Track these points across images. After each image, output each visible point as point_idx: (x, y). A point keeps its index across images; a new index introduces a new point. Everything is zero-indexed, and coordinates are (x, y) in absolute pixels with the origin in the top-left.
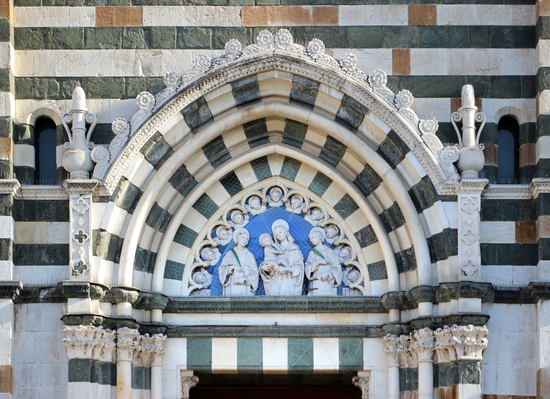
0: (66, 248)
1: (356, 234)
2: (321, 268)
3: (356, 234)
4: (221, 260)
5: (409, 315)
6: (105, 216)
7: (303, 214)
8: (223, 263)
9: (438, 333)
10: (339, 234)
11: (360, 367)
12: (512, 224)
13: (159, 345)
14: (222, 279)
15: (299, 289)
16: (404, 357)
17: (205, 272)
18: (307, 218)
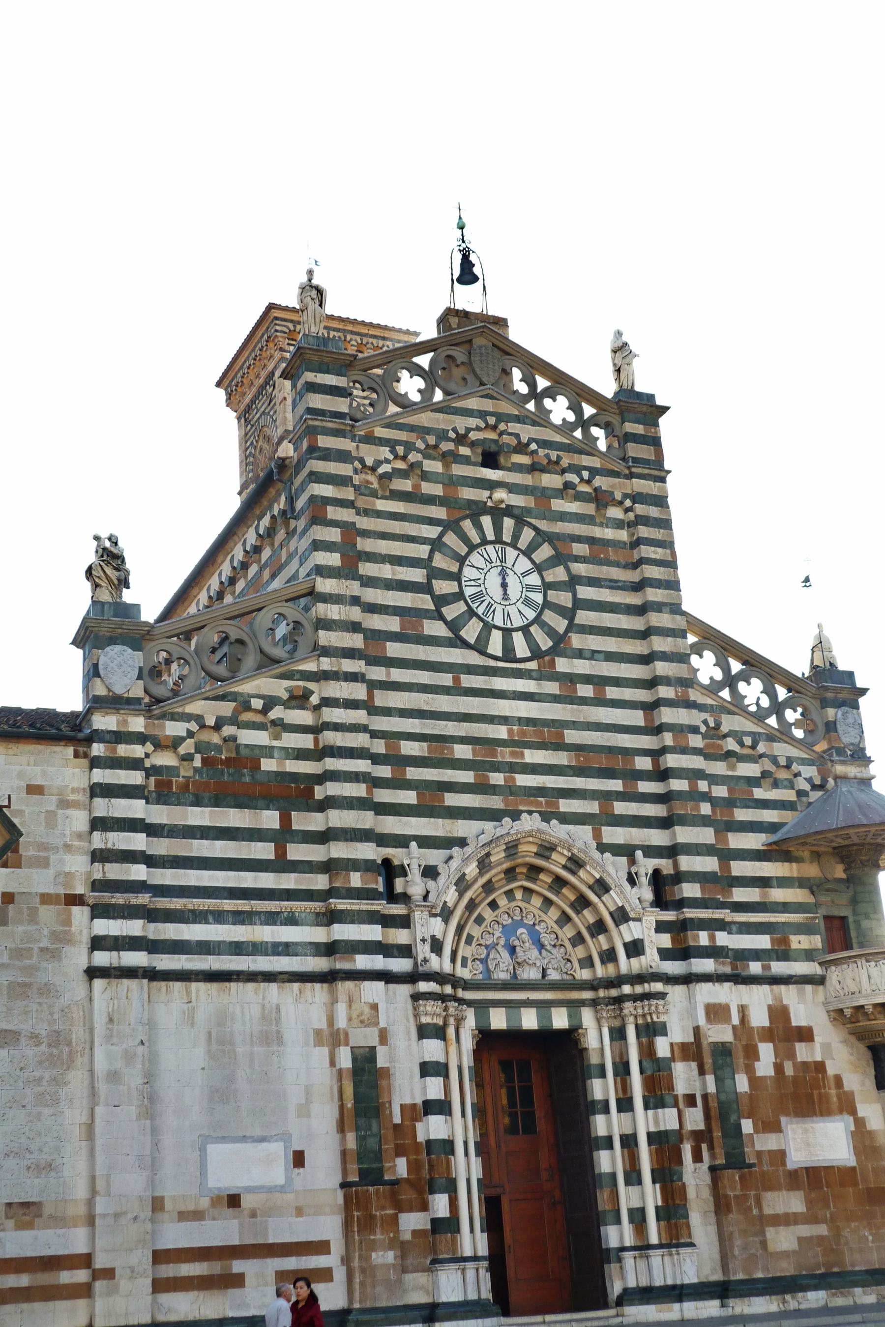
1: (569, 939)
2: (553, 962)
3: (569, 939)
4: (488, 955)
5: (614, 993)
7: (534, 924)
8: (491, 956)
9: (639, 1004)
10: (557, 938)
11: (580, 1026)
12: (669, 935)
14: (491, 967)
15: (539, 976)
16: (611, 1020)
17: (478, 962)
18: (537, 927)
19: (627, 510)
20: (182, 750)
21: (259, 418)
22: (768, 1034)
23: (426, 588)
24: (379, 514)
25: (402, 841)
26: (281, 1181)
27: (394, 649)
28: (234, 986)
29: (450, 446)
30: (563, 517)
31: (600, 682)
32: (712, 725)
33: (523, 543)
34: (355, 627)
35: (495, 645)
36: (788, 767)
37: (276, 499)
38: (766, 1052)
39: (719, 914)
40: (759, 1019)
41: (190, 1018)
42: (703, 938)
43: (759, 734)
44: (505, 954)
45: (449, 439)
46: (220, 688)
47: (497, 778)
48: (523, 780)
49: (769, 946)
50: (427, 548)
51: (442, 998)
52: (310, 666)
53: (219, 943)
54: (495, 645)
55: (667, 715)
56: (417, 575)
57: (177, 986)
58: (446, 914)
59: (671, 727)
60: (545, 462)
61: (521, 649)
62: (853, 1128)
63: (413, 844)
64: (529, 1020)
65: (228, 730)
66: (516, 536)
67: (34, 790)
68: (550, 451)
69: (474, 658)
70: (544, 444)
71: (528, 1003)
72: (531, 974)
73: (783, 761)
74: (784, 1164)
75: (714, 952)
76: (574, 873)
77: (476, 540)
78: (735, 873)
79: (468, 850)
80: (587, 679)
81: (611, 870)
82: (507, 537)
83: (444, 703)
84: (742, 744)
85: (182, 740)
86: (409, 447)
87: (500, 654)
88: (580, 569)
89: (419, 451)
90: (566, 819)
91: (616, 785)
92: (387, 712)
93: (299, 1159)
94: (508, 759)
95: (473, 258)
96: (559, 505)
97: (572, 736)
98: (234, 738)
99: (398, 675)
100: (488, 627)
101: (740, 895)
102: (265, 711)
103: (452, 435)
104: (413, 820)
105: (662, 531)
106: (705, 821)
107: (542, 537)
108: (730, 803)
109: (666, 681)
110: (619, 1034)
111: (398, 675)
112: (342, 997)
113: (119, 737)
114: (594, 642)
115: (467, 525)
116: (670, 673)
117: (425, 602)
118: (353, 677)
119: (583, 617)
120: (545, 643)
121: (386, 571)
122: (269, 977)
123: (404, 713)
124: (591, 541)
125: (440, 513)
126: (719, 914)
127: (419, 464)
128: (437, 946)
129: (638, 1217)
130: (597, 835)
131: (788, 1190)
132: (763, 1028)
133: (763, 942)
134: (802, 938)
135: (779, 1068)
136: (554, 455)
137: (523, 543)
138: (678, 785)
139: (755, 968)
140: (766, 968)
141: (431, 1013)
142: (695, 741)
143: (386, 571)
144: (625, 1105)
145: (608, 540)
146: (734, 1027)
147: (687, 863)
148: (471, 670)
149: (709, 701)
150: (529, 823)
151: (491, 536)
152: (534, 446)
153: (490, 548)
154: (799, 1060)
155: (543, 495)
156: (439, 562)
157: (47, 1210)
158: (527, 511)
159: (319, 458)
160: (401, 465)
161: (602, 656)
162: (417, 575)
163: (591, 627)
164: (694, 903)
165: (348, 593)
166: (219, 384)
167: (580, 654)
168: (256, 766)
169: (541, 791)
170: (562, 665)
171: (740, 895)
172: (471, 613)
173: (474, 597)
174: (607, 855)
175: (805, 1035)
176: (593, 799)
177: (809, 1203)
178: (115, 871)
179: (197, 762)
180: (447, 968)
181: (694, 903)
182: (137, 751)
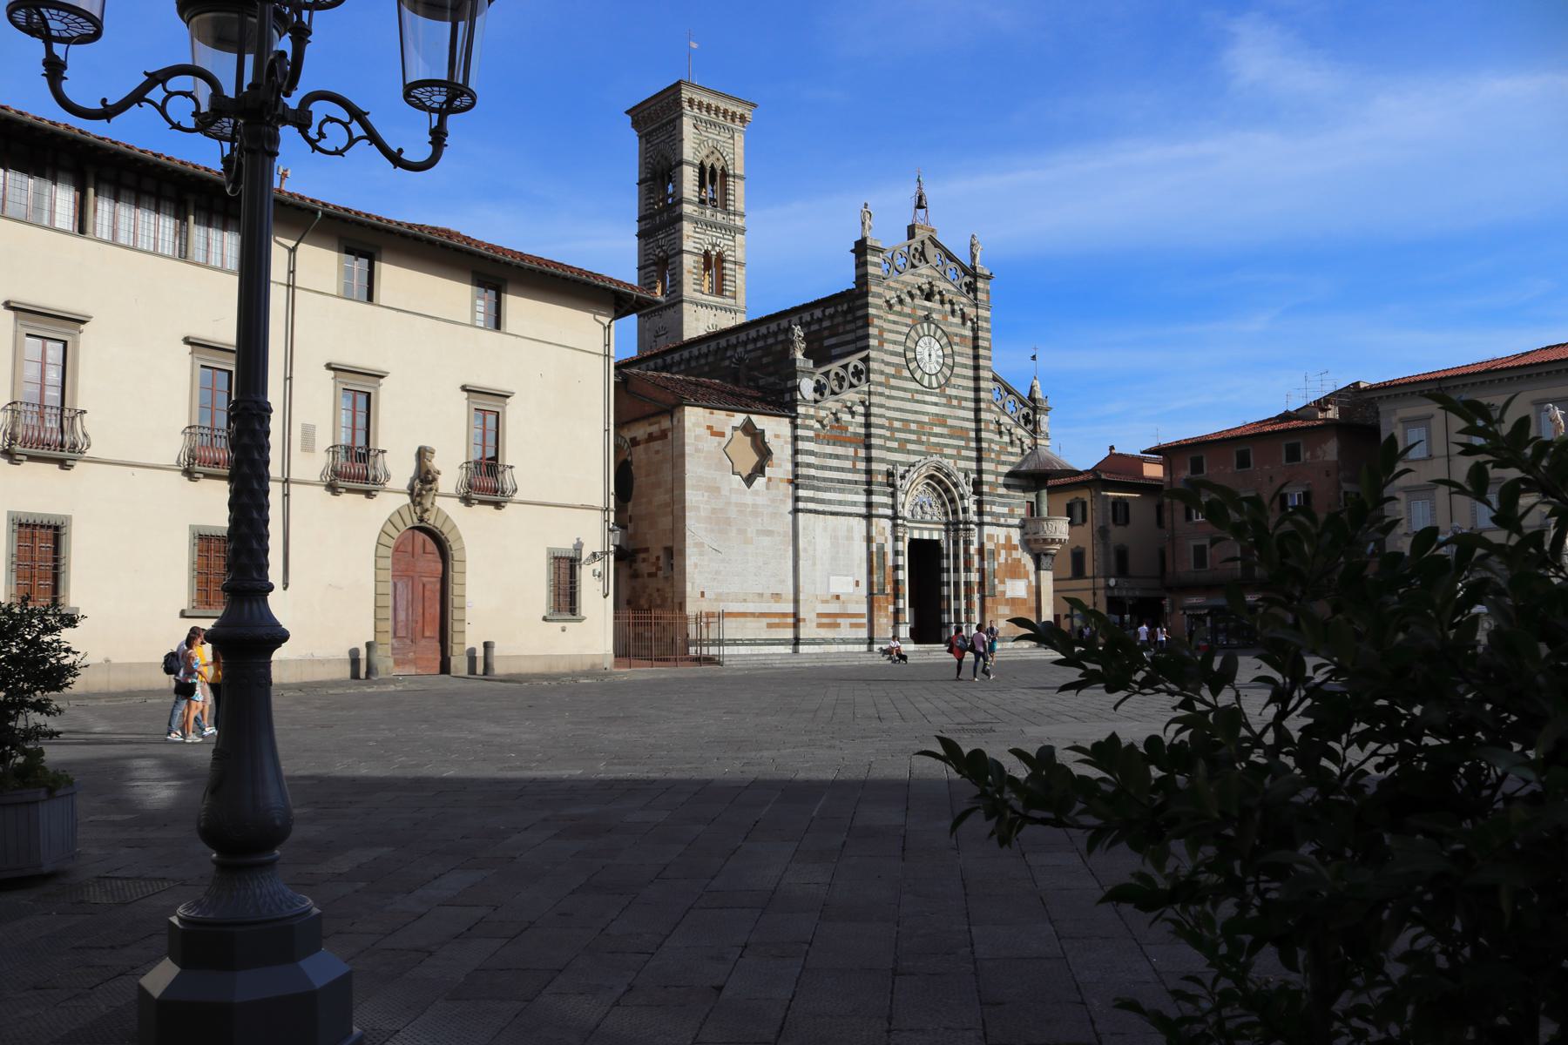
19: (973, 323)
21: (657, 143)
22: (1004, 547)
24: (889, 321)
25: (894, 463)
27: (893, 382)
30: (951, 324)
34: (882, 373)
35: (926, 383)
37: (842, 304)
38: (1003, 552)
40: (1002, 541)
41: (825, 529)
44: (919, 508)
46: (836, 397)
47: (924, 438)
48: (933, 439)
52: (866, 389)
53: (835, 500)
56: (900, 349)
57: (821, 516)
64: (926, 536)
66: (935, 333)
67: (777, 436)
70: (948, 291)
71: (926, 529)
72: (928, 517)
75: (991, 514)
77: (922, 334)
79: (916, 468)
80: (956, 397)
83: (908, 406)
85: (825, 418)
90: (946, 456)
91: (962, 443)
92: (889, 408)
93: (857, 584)
95: (924, 198)
97: (950, 422)
99: (894, 393)
104: (896, 454)
106: (992, 461)
110: (956, 543)
111: (894, 393)
112: (874, 524)
113: (807, 416)
115: (919, 326)
118: (881, 394)
120: (943, 381)
122: (850, 515)
125: (909, 321)
129: (957, 612)
130: (955, 464)
133: (1005, 510)
135: (1006, 560)
139: (1002, 521)
140: (1006, 520)
144: (956, 570)
148: (917, 392)
150: (936, 458)
151: (926, 333)
153: (926, 338)
157: (783, 596)
159: (872, 297)
166: (627, 112)
167: (954, 386)
168: (847, 430)
169: (938, 444)
170: (948, 391)
175: (1015, 548)
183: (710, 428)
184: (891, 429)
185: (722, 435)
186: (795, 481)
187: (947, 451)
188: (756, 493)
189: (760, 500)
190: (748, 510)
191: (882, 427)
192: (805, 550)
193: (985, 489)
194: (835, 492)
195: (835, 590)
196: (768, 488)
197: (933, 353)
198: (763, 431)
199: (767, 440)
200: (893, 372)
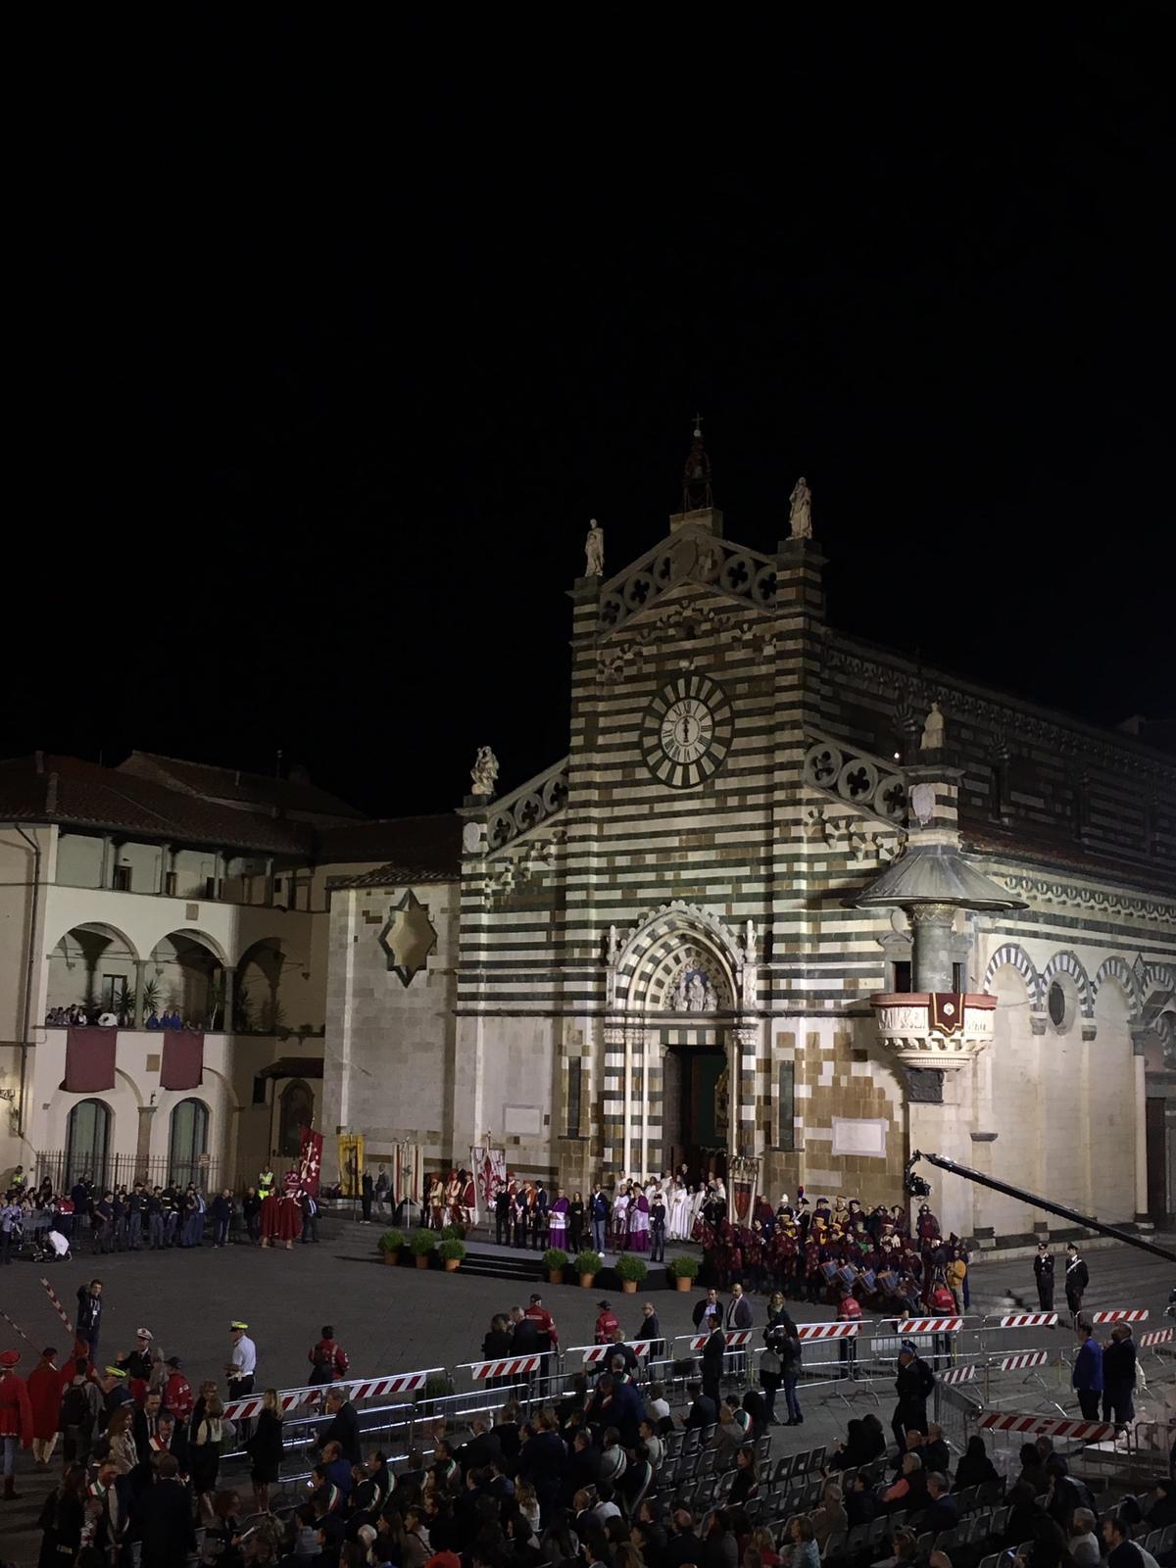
0: (605, 993)
6: (619, 981)
13: (646, 1035)
20: (502, 880)
22: (831, 1055)
23: (638, 745)
26: (537, 1131)
27: (618, 794)
28: (522, 1018)
29: (662, 634)
31: (742, 792)
32: (816, 814)
33: (702, 697)
34: (588, 785)
35: (677, 780)
36: (874, 839)
38: (828, 1067)
39: (795, 966)
40: (827, 1043)
42: (782, 984)
43: (852, 816)
45: (661, 629)
47: (669, 876)
48: (686, 875)
49: (842, 988)
50: (641, 714)
51: (624, 1027)
54: (677, 780)
55: (780, 814)
56: (633, 737)
57: (498, 1019)
58: (630, 971)
59: (778, 823)
60: (717, 625)
61: (694, 777)
62: (887, 1130)
63: (613, 928)
64: (692, 1039)
65: (523, 865)
66: (699, 690)
68: (722, 616)
69: (664, 790)
70: (718, 611)
71: (692, 1027)
72: (697, 1007)
73: (869, 837)
74: (830, 1152)
75: (791, 995)
76: (711, 939)
78: (823, 931)
81: (726, 938)
82: (692, 694)
83: (644, 826)
84: (837, 827)
85: (502, 873)
86: (632, 642)
87: (680, 784)
88: (739, 705)
89: (641, 644)
94: (678, 861)
96: (730, 656)
97: (720, 838)
98: (527, 869)
99: (618, 811)
100: (675, 764)
101: (826, 948)
102: (542, 848)
103: (659, 624)
105: (793, 660)
107: (717, 685)
108: (827, 875)
109: (781, 786)
111: (618, 811)
112: (565, 1026)
114: (743, 762)
115: (669, 690)
116: (784, 780)
117: (634, 755)
118: (587, 820)
119: (738, 743)
121: (616, 738)
123: (619, 837)
124: (750, 679)
125: (652, 685)
126: (795, 966)
127: (639, 654)
128: (623, 993)
130: (729, 909)
131: (831, 1169)
132: (829, 1050)
133: (838, 984)
134: (868, 980)
135: (836, 1081)
136: (724, 617)
137: (702, 697)
138: (779, 868)
140: (835, 1004)
141: (616, 1037)
142: (795, 831)
143: (616, 738)
145: (763, 676)
146: (796, 1050)
147: (779, 928)
149: (817, 795)
151: (682, 695)
152: (712, 615)
153: (681, 704)
154: (853, 1074)
155: (718, 650)
156: (651, 723)
158: (708, 668)
160: (629, 656)
161: (746, 772)
162: (633, 737)
163: (743, 750)
164: (781, 959)
165: (585, 762)
167: (733, 773)
169: (695, 882)
170: (720, 784)
171: (826, 948)
172: (665, 757)
173: (667, 744)
174: (724, 926)
176: (729, 883)
177: (845, 1182)
178: (467, 956)
179: (513, 886)
180: (635, 1005)
181: (781, 959)
182: (482, 884)
183: (366, 913)
184: (613, 871)
185: (378, 920)
186: (461, 972)
187: (711, 890)
188: (415, 993)
189: (418, 1002)
190: (406, 1015)
191: (586, 871)
192: (462, 1069)
193: (779, 949)
194: (518, 981)
195: (513, 1129)
196: (429, 982)
197: (693, 727)
198: (426, 907)
199: (431, 919)
200: (619, 779)
